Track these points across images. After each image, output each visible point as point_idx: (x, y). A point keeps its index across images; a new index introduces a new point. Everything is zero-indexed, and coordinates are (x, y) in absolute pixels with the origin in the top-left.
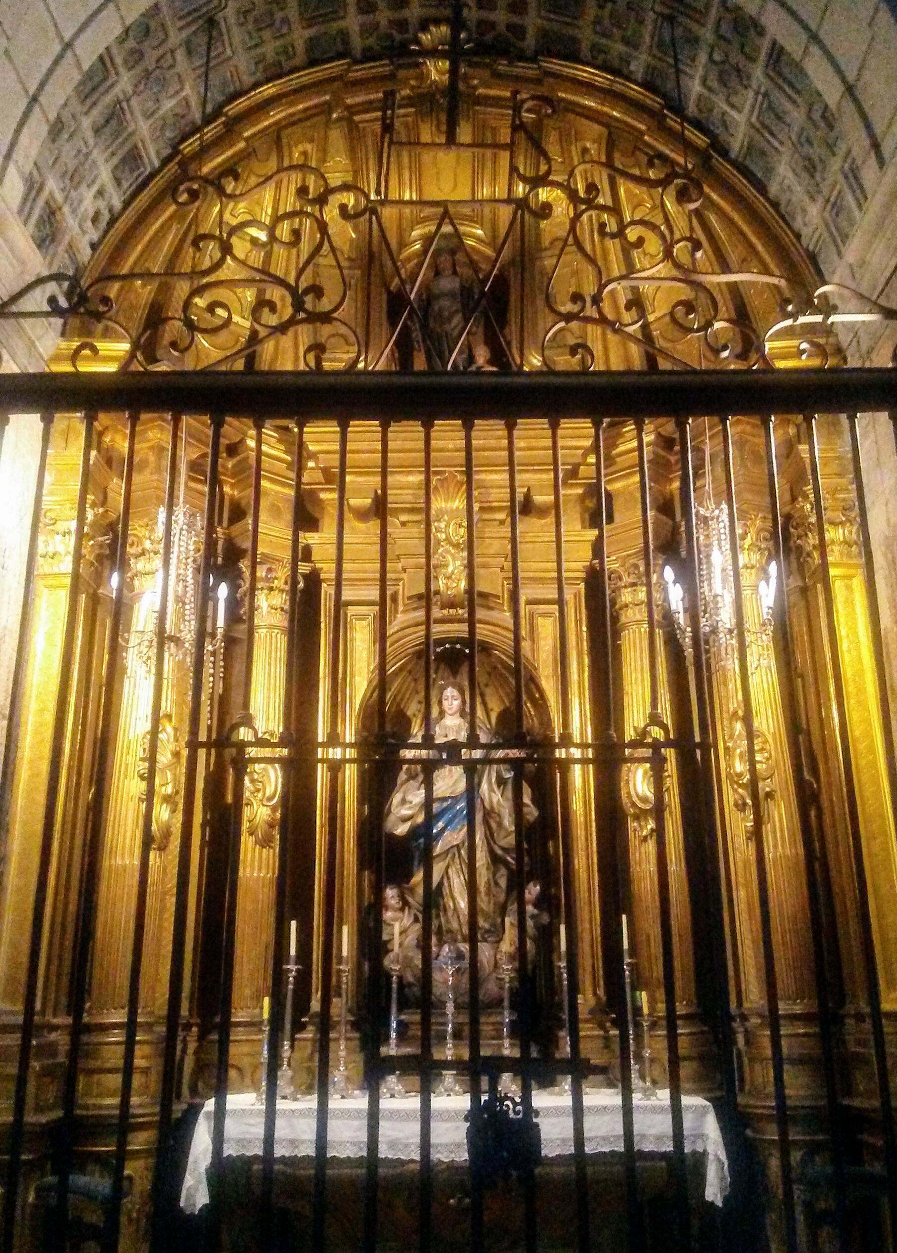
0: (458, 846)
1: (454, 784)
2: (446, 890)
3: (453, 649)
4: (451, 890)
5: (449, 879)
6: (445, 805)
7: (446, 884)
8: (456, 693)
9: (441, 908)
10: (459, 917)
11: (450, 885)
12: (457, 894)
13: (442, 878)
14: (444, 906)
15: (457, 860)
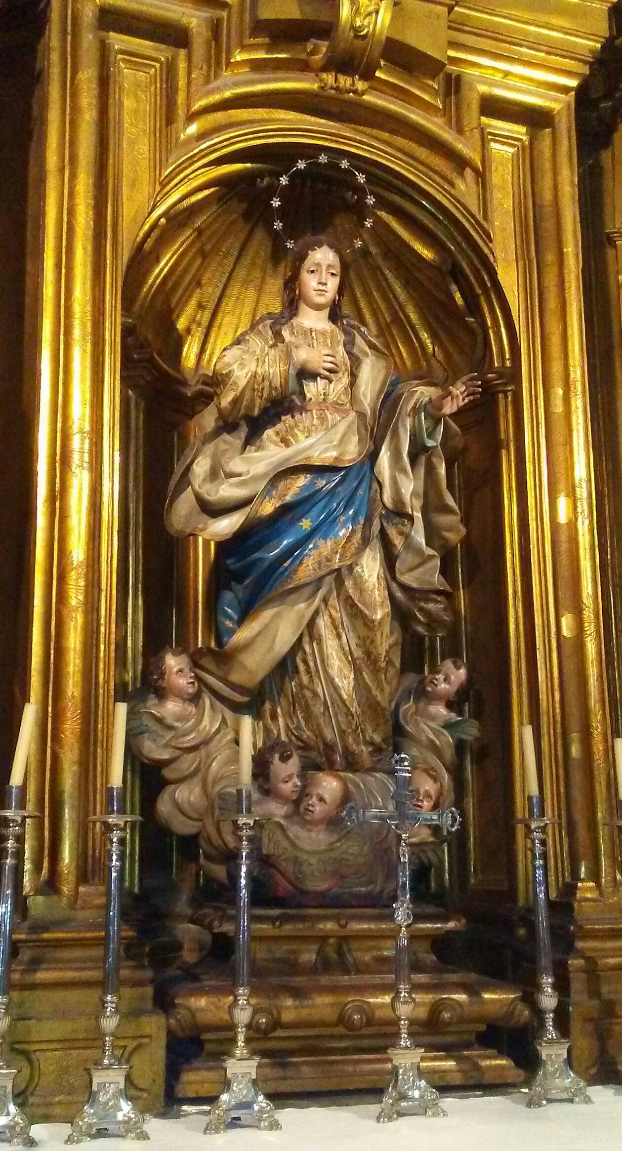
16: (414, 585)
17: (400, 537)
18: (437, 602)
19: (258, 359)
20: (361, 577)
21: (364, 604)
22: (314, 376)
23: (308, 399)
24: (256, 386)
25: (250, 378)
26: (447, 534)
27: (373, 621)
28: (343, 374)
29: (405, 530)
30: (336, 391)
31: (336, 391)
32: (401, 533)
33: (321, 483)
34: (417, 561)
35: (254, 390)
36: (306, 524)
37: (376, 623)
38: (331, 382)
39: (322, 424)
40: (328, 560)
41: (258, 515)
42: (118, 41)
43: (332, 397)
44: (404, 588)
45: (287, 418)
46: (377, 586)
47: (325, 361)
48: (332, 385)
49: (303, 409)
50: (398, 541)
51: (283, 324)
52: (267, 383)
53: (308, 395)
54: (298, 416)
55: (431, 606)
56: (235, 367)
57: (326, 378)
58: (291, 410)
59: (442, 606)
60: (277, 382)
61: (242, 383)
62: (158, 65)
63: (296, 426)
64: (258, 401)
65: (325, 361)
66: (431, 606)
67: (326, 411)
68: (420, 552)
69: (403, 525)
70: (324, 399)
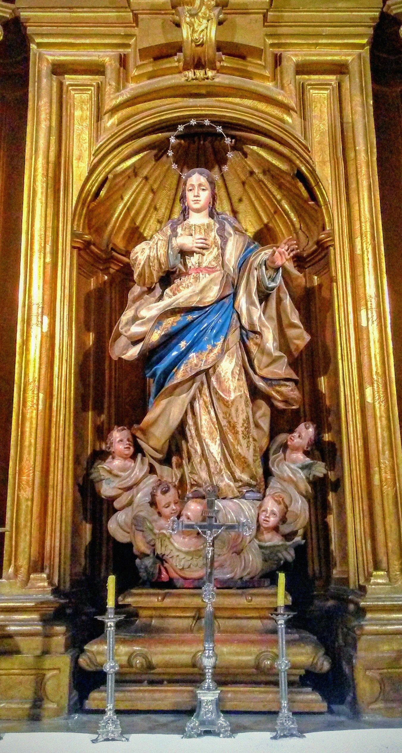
0: (206, 372)
1: (201, 291)
2: (191, 431)
3: (200, 125)
4: (197, 430)
5: (194, 413)
6: (189, 318)
7: (190, 422)
8: (203, 180)
9: (185, 455)
10: (208, 465)
11: (196, 424)
12: (205, 435)
13: (186, 413)
14: (189, 452)
15: (206, 391)
16: (270, 376)
17: (255, 347)
18: (287, 386)
19: (150, 248)
20: (220, 374)
21: (223, 391)
22: (191, 253)
23: (189, 267)
24: (151, 264)
25: (146, 259)
26: (297, 342)
27: (227, 402)
28: (213, 248)
29: (258, 341)
30: (208, 260)
31: (208, 260)
32: (256, 344)
33: (189, 318)
34: (270, 361)
35: (150, 266)
36: (183, 345)
37: (230, 403)
38: (203, 255)
39: (196, 281)
40: (196, 365)
41: (151, 341)
42: (69, 79)
43: (204, 265)
44: (264, 378)
45: (177, 281)
46: (231, 378)
47: (197, 243)
48: (205, 257)
49: (187, 274)
50: (254, 349)
51: (179, 225)
52: (156, 261)
53: (189, 265)
54: (183, 278)
55: (283, 389)
56: (139, 254)
57: (199, 253)
58: (180, 275)
59: (290, 388)
60: (163, 260)
61: (142, 263)
62: (93, 88)
63: (181, 284)
64: (155, 273)
65: (197, 243)
66: (283, 389)
67: (201, 274)
68: (269, 354)
69: (257, 338)
70: (199, 266)
